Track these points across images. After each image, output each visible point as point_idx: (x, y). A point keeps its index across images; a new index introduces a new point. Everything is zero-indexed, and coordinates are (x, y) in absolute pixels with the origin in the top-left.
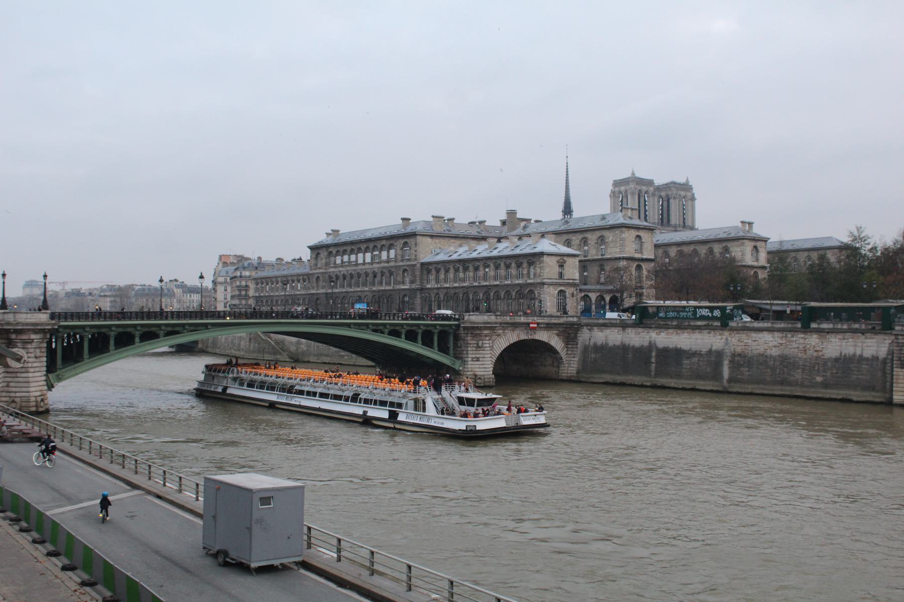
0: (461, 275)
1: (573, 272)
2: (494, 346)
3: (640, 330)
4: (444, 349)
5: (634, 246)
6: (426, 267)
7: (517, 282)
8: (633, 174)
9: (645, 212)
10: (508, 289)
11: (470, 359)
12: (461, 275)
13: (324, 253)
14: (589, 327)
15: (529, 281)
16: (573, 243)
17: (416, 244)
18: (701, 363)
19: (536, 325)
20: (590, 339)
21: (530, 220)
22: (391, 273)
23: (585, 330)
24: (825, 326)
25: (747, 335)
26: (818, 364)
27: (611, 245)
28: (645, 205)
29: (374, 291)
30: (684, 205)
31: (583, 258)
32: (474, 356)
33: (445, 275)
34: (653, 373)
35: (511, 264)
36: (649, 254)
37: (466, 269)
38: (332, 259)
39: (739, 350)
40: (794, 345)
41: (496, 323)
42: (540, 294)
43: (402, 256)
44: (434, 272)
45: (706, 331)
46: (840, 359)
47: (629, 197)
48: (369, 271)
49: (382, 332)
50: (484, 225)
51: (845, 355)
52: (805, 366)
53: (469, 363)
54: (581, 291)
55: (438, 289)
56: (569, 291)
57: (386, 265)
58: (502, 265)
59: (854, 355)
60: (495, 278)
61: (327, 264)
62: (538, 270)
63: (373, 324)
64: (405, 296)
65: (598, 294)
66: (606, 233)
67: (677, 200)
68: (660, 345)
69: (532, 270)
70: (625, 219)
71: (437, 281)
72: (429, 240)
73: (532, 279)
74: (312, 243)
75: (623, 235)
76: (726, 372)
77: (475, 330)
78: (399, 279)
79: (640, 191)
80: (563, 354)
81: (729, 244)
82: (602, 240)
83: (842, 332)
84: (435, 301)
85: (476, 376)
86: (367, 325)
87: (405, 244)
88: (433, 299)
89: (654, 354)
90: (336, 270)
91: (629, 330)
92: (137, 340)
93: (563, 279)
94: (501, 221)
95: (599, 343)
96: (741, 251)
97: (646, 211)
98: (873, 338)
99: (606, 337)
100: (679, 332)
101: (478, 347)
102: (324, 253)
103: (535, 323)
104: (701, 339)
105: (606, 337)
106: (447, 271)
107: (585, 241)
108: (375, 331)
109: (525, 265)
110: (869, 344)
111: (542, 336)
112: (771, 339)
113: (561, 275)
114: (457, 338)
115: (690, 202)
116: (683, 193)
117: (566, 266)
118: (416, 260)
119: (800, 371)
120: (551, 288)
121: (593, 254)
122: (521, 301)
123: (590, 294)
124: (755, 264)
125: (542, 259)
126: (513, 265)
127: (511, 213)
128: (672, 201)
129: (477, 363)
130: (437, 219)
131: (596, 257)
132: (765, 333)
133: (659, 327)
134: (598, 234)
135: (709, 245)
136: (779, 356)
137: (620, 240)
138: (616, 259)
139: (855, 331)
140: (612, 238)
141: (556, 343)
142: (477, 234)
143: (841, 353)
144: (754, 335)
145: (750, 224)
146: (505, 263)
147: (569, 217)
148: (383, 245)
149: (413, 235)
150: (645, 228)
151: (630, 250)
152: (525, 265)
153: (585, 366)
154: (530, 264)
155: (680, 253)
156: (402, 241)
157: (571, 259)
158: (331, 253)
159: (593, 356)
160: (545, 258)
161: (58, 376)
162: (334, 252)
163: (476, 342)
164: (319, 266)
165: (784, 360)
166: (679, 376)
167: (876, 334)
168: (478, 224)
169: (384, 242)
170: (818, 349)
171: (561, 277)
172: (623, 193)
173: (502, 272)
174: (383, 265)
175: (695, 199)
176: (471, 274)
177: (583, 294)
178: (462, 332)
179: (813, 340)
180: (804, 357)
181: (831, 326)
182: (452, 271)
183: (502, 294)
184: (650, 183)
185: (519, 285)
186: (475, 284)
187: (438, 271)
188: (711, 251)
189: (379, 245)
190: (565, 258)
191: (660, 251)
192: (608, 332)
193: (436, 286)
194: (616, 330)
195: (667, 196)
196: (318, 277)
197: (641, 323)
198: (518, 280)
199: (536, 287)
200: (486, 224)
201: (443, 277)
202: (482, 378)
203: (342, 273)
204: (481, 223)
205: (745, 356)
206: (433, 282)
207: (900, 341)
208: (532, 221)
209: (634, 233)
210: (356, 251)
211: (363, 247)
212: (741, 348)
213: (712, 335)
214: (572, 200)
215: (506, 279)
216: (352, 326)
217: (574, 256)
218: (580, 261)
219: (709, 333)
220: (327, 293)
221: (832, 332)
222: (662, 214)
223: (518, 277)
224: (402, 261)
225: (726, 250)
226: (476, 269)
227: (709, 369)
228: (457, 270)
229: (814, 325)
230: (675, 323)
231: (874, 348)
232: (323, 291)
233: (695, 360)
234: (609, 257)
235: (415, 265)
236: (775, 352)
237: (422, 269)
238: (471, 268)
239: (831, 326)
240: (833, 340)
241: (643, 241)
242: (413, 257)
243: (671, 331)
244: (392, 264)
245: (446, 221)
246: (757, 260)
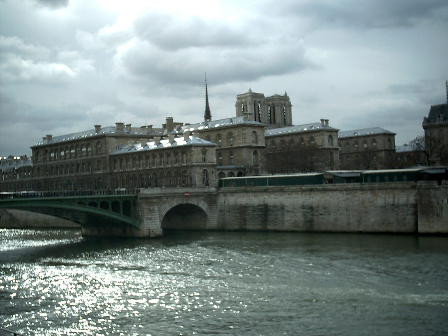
0: (138, 162)
1: (212, 158)
2: (161, 210)
5: (251, 138)
6: (114, 158)
7: (175, 165)
8: (250, 90)
10: (169, 171)
11: (145, 219)
12: (138, 162)
13: (42, 152)
14: (224, 194)
15: (184, 165)
16: (211, 138)
17: (106, 143)
20: (225, 201)
21: (183, 124)
22: (89, 164)
23: (221, 195)
27: (237, 138)
30: (284, 110)
31: (218, 148)
33: (127, 163)
35: (170, 153)
36: (261, 143)
37: (140, 158)
38: (48, 155)
41: (162, 194)
42: (190, 173)
43: (97, 151)
44: (118, 161)
45: (299, 193)
47: (248, 106)
49: (84, 204)
50: (152, 128)
53: (145, 221)
54: (218, 169)
55: (122, 172)
56: (209, 170)
57: (86, 158)
58: (165, 155)
61: (45, 159)
62: (189, 157)
63: (78, 199)
64: (100, 178)
65: (229, 171)
66: (233, 131)
67: (280, 107)
69: (185, 156)
70: (245, 121)
71: (121, 167)
72: (114, 140)
73: (185, 163)
74: (33, 145)
75: (244, 132)
77: (148, 199)
78: (95, 167)
79: (255, 101)
80: (208, 214)
81: (313, 135)
82: (230, 135)
84: (120, 180)
85: (149, 230)
86: (74, 200)
87: (98, 143)
88: (119, 180)
90: (51, 163)
93: (206, 162)
94: (163, 125)
96: (321, 139)
100: (282, 194)
101: (150, 210)
106: (128, 160)
107: (219, 136)
109: (180, 154)
111: (194, 201)
112: (342, 195)
113: (204, 160)
114: (135, 204)
115: (288, 107)
116: (283, 102)
117: (208, 154)
118: (106, 153)
121: (225, 145)
122: (179, 178)
123: (224, 172)
124: (331, 147)
125: (191, 149)
127: (170, 120)
128: (276, 107)
129: (150, 221)
130: (119, 125)
131: (227, 147)
132: (338, 192)
134: (228, 131)
135: (300, 136)
137: (243, 135)
138: (240, 147)
140: (237, 134)
141: (203, 205)
142: (147, 134)
143: (385, 203)
144: (330, 193)
145: (327, 121)
146: (166, 153)
147: (209, 120)
149: (104, 136)
150: (258, 126)
151: (249, 141)
152: (180, 154)
154: (183, 153)
155: (283, 142)
156: (96, 141)
157: (210, 149)
160: (193, 149)
162: (49, 151)
163: (149, 207)
164: (39, 160)
168: (147, 127)
171: (205, 161)
172: (244, 103)
173: (165, 159)
174: (83, 158)
175: (291, 106)
176: (144, 162)
177: (219, 172)
182: (131, 160)
183: (165, 174)
184: (262, 96)
185: (176, 167)
186: (147, 168)
187: (121, 161)
188: (302, 140)
189: (80, 144)
190: (206, 148)
191: (269, 142)
193: (121, 171)
195: (273, 104)
196: (39, 169)
198: (175, 164)
200: (153, 127)
201: (125, 164)
202: (154, 231)
203: (55, 165)
204: (149, 127)
208: (184, 125)
209: (251, 130)
210: (64, 149)
211: (69, 146)
213: (304, 195)
214: (211, 109)
217: (212, 146)
218: (216, 150)
220: (45, 179)
222: (270, 117)
223: (175, 162)
224: (97, 154)
225: (312, 139)
226: (147, 158)
228: (134, 159)
232: (41, 178)
234: (236, 146)
235: (106, 157)
237: (110, 159)
238: (144, 157)
240: (380, 194)
241: (258, 135)
242: (104, 152)
244: (90, 157)
245: (126, 127)
246: (332, 144)
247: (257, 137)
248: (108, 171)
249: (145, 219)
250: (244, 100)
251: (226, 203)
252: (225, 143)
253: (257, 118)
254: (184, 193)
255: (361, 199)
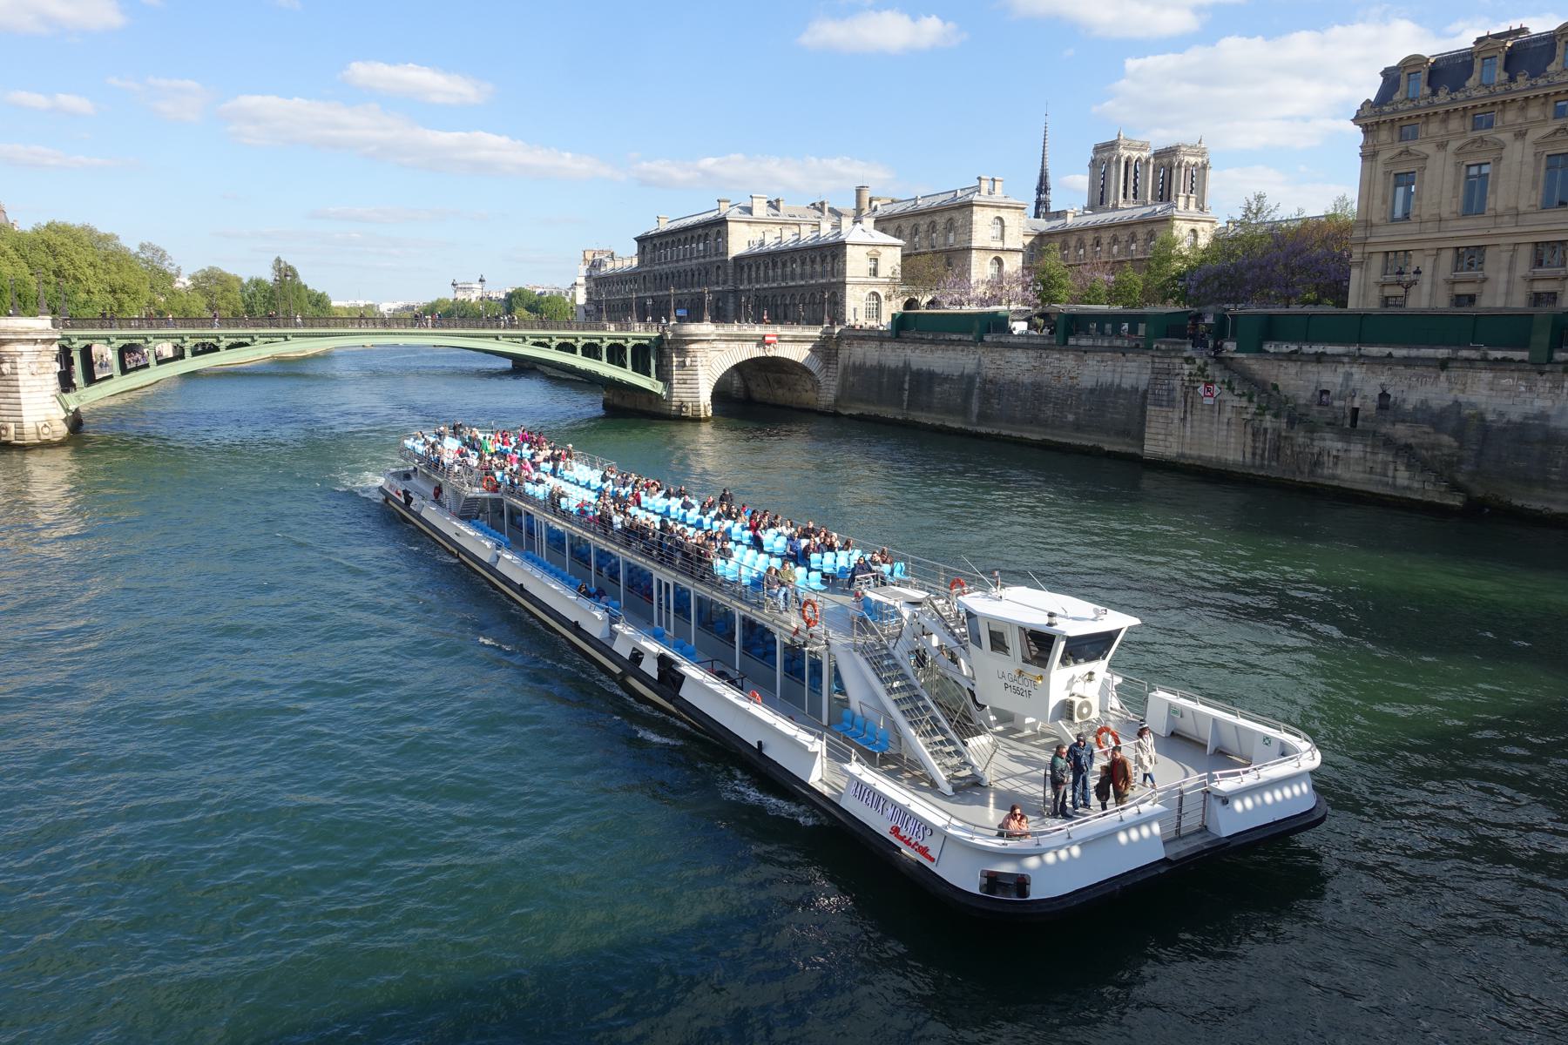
3: (897, 345)
4: (641, 367)
9: (1135, 188)
18: (952, 391)
19: (775, 339)
24: (1084, 342)
25: (1000, 355)
26: (1072, 396)
27: (960, 231)
28: (1136, 177)
29: (692, 294)
32: (680, 377)
33: (757, 272)
34: (905, 404)
35: (815, 257)
39: (991, 374)
40: (1048, 369)
45: (960, 348)
46: (1095, 390)
48: (688, 269)
49: (549, 347)
51: (1102, 385)
52: (1058, 399)
59: (1112, 384)
60: (802, 277)
61: (652, 260)
66: (956, 215)
68: (914, 367)
72: (744, 226)
76: (975, 406)
78: (714, 279)
80: (820, 377)
81: (1155, 227)
83: (1101, 352)
89: (907, 378)
91: (887, 345)
92: (188, 353)
95: (857, 363)
97: (1136, 185)
98: (1134, 361)
99: (865, 354)
102: (649, 247)
103: (773, 336)
104: (956, 359)
105: (865, 354)
108: (534, 344)
110: (1130, 369)
112: (1025, 360)
119: (1051, 405)
120: (858, 288)
126: (818, 258)
132: (1019, 350)
133: (914, 341)
134: (947, 215)
135: (1131, 230)
136: (1032, 384)
139: (1113, 349)
144: (1008, 354)
148: (700, 236)
152: (829, 259)
153: (845, 394)
156: (715, 230)
158: (655, 245)
159: (851, 379)
161: (78, 396)
165: (1038, 392)
166: (929, 408)
167: (1138, 354)
169: (700, 231)
170: (1073, 375)
174: (702, 260)
178: (667, 346)
179: (1069, 362)
180: (1058, 386)
181: (1090, 342)
192: (866, 347)
194: (874, 344)
197: (898, 336)
199: (838, 288)
202: (690, 404)
205: (997, 384)
206: (746, 282)
207: (1156, 365)
209: (993, 213)
211: (682, 237)
212: (993, 371)
215: (812, 278)
216: (500, 338)
219: (963, 351)
221: (1090, 351)
224: (716, 255)
227: (959, 400)
229: (1072, 341)
230: (930, 337)
231: (1134, 376)
233: (946, 386)
236: (1027, 379)
239: (1090, 342)
240: (1090, 362)
243: (925, 347)
247: (1003, 227)
248: (729, 286)
249: (675, 381)
250: (1106, 154)
251: (851, 360)
252: (941, 240)
253: (1131, 192)
254: (764, 337)
255: (1055, 371)
